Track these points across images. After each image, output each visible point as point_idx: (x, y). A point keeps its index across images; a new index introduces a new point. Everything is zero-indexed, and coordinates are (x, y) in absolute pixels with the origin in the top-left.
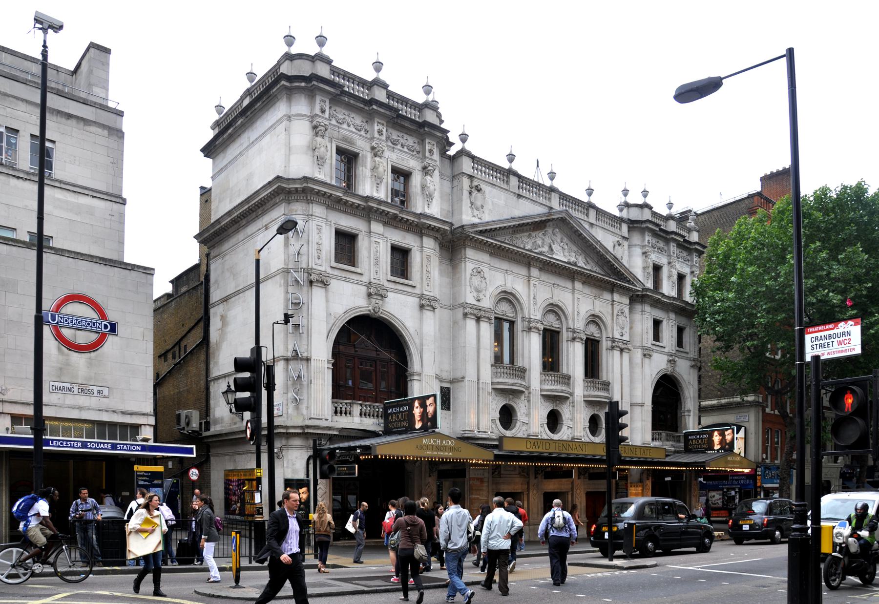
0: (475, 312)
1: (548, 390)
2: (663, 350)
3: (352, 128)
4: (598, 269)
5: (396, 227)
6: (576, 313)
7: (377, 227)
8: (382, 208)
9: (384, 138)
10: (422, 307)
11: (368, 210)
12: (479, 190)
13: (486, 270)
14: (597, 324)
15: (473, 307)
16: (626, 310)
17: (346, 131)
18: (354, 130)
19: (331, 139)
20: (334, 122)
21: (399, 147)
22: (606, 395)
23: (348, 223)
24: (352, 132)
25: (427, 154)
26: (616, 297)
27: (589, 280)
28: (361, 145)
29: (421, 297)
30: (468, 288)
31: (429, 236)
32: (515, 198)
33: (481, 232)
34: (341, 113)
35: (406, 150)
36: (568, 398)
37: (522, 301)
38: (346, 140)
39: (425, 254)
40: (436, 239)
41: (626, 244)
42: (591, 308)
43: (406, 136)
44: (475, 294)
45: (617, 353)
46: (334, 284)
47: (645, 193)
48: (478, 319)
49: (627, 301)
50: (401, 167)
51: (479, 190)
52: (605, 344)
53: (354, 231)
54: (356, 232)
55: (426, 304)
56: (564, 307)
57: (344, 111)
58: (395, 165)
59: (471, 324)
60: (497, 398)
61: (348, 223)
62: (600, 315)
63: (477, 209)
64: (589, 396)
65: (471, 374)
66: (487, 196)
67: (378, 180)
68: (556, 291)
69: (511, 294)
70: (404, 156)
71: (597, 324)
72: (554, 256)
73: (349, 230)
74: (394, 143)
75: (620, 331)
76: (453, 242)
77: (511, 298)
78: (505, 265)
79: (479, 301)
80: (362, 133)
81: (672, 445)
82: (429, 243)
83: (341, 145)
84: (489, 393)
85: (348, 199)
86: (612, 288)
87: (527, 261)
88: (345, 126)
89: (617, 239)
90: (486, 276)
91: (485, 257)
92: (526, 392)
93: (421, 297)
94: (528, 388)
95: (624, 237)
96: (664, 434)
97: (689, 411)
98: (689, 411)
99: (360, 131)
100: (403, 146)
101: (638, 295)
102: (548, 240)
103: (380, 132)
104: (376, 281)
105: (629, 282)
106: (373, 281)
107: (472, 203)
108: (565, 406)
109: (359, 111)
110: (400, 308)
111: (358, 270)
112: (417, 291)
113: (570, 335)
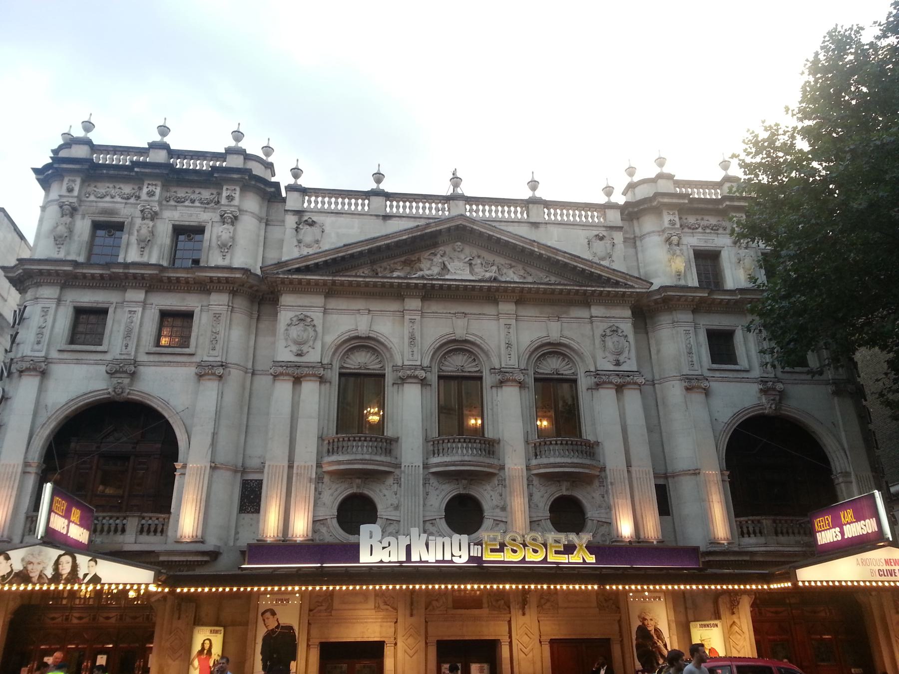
0: (290, 370)
1: (438, 465)
2: (745, 375)
3: (118, 199)
4: (553, 279)
5: (169, 290)
6: (503, 346)
8: (132, 271)
9: (156, 198)
10: (200, 376)
11: (122, 279)
12: (312, 224)
13: (317, 316)
14: (564, 356)
15: (287, 365)
16: (627, 327)
18: (119, 200)
19: (83, 217)
20: (92, 198)
21: (186, 203)
22: (587, 462)
23: (89, 298)
24: (114, 202)
25: (224, 201)
26: (597, 311)
27: (522, 297)
28: (126, 211)
29: (199, 365)
31: (220, 291)
32: (380, 221)
33: (298, 271)
34: (102, 188)
35: (197, 204)
36: (492, 475)
37: (389, 345)
38: (105, 212)
39: (213, 315)
40: (234, 293)
41: (618, 237)
43: (197, 190)
44: (295, 348)
45: (607, 395)
46: (58, 370)
47: (661, 162)
48: (297, 381)
49: (628, 313)
50: (187, 223)
51: (312, 224)
53: (100, 305)
54: (105, 306)
55: (210, 372)
56: (478, 341)
57: (107, 185)
58: (177, 223)
59: (284, 388)
60: (334, 486)
61: (89, 298)
62: (564, 341)
63: (308, 246)
64: (539, 466)
65: (276, 456)
67: (145, 244)
68: (460, 323)
69: (369, 338)
70: (192, 211)
71: (564, 356)
72: (447, 277)
73: (95, 305)
74: (179, 201)
75: (612, 358)
76: (261, 293)
77: (371, 344)
78: (360, 304)
79: (299, 355)
80: (132, 200)
81: (798, 543)
82: (219, 301)
83: (97, 219)
85: (85, 271)
86: (585, 301)
87: (397, 293)
88: (108, 199)
89: (596, 233)
90: (315, 322)
91: (319, 300)
92: (397, 472)
93: (199, 365)
94: (398, 466)
95: (612, 228)
96: (767, 522)
97: (846, 474)
98: (846, 474)
99: (128, 198)
100: (193, 201)
101: (656, 301)
102: (438, 259)
103: (151, 194)
104: (123, 357)
105: (617, 284)
106: (118, 357)
107: (300, 242)
108: (488, 487)
109: (127, 179)
110: (167, 386)
111: (99, 348)
112: (196, 359)
113: (592, 380)
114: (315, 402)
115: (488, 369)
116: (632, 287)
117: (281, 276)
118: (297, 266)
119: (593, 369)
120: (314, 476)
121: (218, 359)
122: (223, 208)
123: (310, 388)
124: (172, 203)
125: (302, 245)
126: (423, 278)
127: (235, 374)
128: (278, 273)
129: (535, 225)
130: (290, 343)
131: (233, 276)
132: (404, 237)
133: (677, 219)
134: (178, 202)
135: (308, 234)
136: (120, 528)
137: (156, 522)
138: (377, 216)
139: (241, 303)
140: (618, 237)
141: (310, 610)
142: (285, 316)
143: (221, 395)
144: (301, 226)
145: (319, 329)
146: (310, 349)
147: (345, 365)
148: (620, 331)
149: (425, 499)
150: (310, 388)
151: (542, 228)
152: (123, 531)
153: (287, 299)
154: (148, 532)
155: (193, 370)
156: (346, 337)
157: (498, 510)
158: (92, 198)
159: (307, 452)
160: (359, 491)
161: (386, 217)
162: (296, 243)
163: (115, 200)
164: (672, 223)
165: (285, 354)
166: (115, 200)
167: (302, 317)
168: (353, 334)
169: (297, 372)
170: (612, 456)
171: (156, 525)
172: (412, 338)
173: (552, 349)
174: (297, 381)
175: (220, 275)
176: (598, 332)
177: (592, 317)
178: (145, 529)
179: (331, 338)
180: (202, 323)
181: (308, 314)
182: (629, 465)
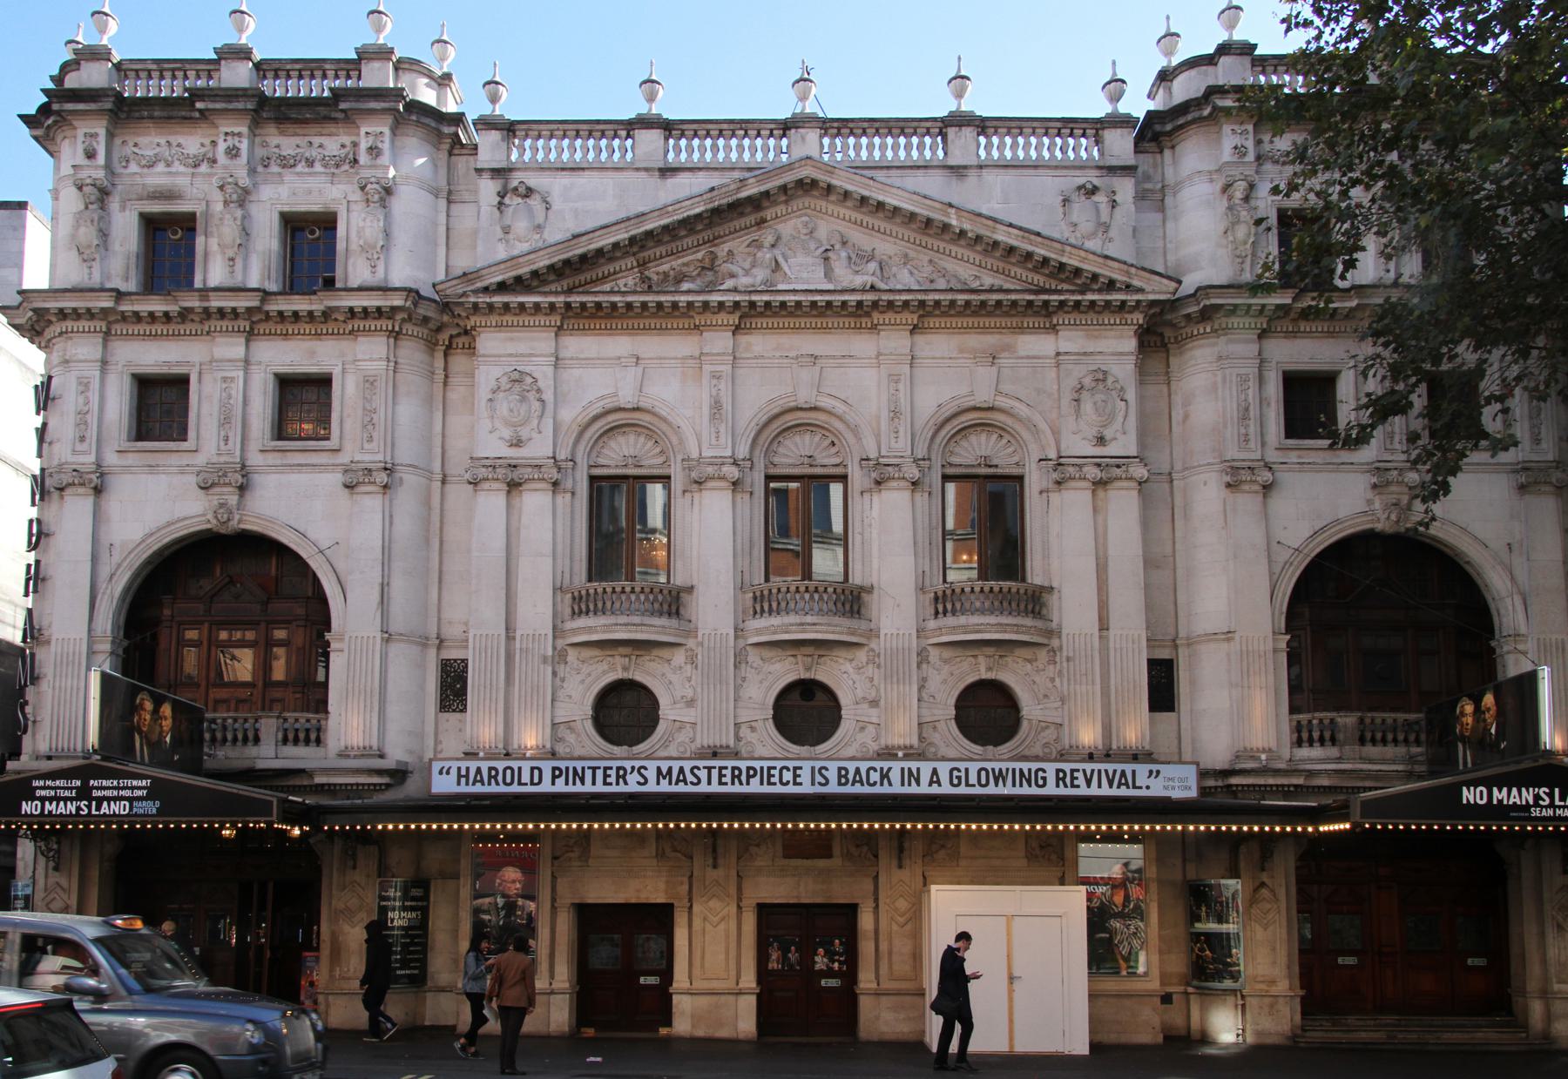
1: (759, 632)
3: (178, 167)
7: (231, 348)
17: (157, 178)
18: (182, 169)
21: (299, 168)
23: (157, 356)
28: (198, 192)
30: (486, 424)
32: (654, 180)
33: (502, 287)
42: (964, 390)
43: (317, 140)
45: (1077, 499)
48: (513, 486)
49: (1131, 344)
52: (1035, 481)
56: (840, 408)
59: (492, 502)
66: (557, 205)
72: (781, 287)
74: (287, 163)
77: (644, 418)
80: (204, 168)
84: (545, 660)
88: (160, 167)
89: (1081, 181)
90: (541, 384)
100: (310, 163)
103: (233, 153)
104: (222, 459)
105: (1111, 285)
106: (215, 460)
110: (297, 503)
112: (344, 458)
114: (550, 529)
115: (856, 460)
116: (1140, 290)
117: (472, 299)
118: (499, 278)
119: (1053, 455)
120: (550, 653)
121: (380, 457)
122: (366, 173)
123: (536, 502)
124: (275, 169)
125: (511, 236)
126: (735, 290)
127: (410, 481)
128: (464, 294)
129: (958, 171)
130: (498, 424)
131: (389, 303)
132: (697, 211)
133: (1250, 144)
134: (284, 167)
135: (520, 217)
136: (251, 735)
137: (308, 726)
138: (646, 170)
139: (411, 352)
140: (1125, 189)
141: (555, 858)
142: (488, 375)
143: (389, 520)
144: (507, 200)
145: (548, 396)
146: (534, 435)
147: (601, 461)
148: (1110, 380)
149: (737, 688)
150: (536, 502)
151: (972, 175)
152: (257, 740)
153: (491, 342)
154: (296, 741)
155: (337, 478)
156: (597, 409)
157: (866, 706)
158: (133, 168)
159: (537, 611)
160: (626, 676)
161: (667, 171)
162: (499, 233)
163: (173, 169)
164: (1239, 151)
165: (493, 446)
166: (173, 169)
167: (516, 376)
168: (609, 403)
169: (515, 475)
170: (1074, 612)
171: (308, 731)
172: (717, 406)
173: (977, 419)
174: (513, 486)
175: (365, 303)
176: (1071, 382)
177: (1058, 354)
178: (291, 736)
179: (571, 414)
180: (345, 393)
181: (527, 369)
182: (1104, 626)
